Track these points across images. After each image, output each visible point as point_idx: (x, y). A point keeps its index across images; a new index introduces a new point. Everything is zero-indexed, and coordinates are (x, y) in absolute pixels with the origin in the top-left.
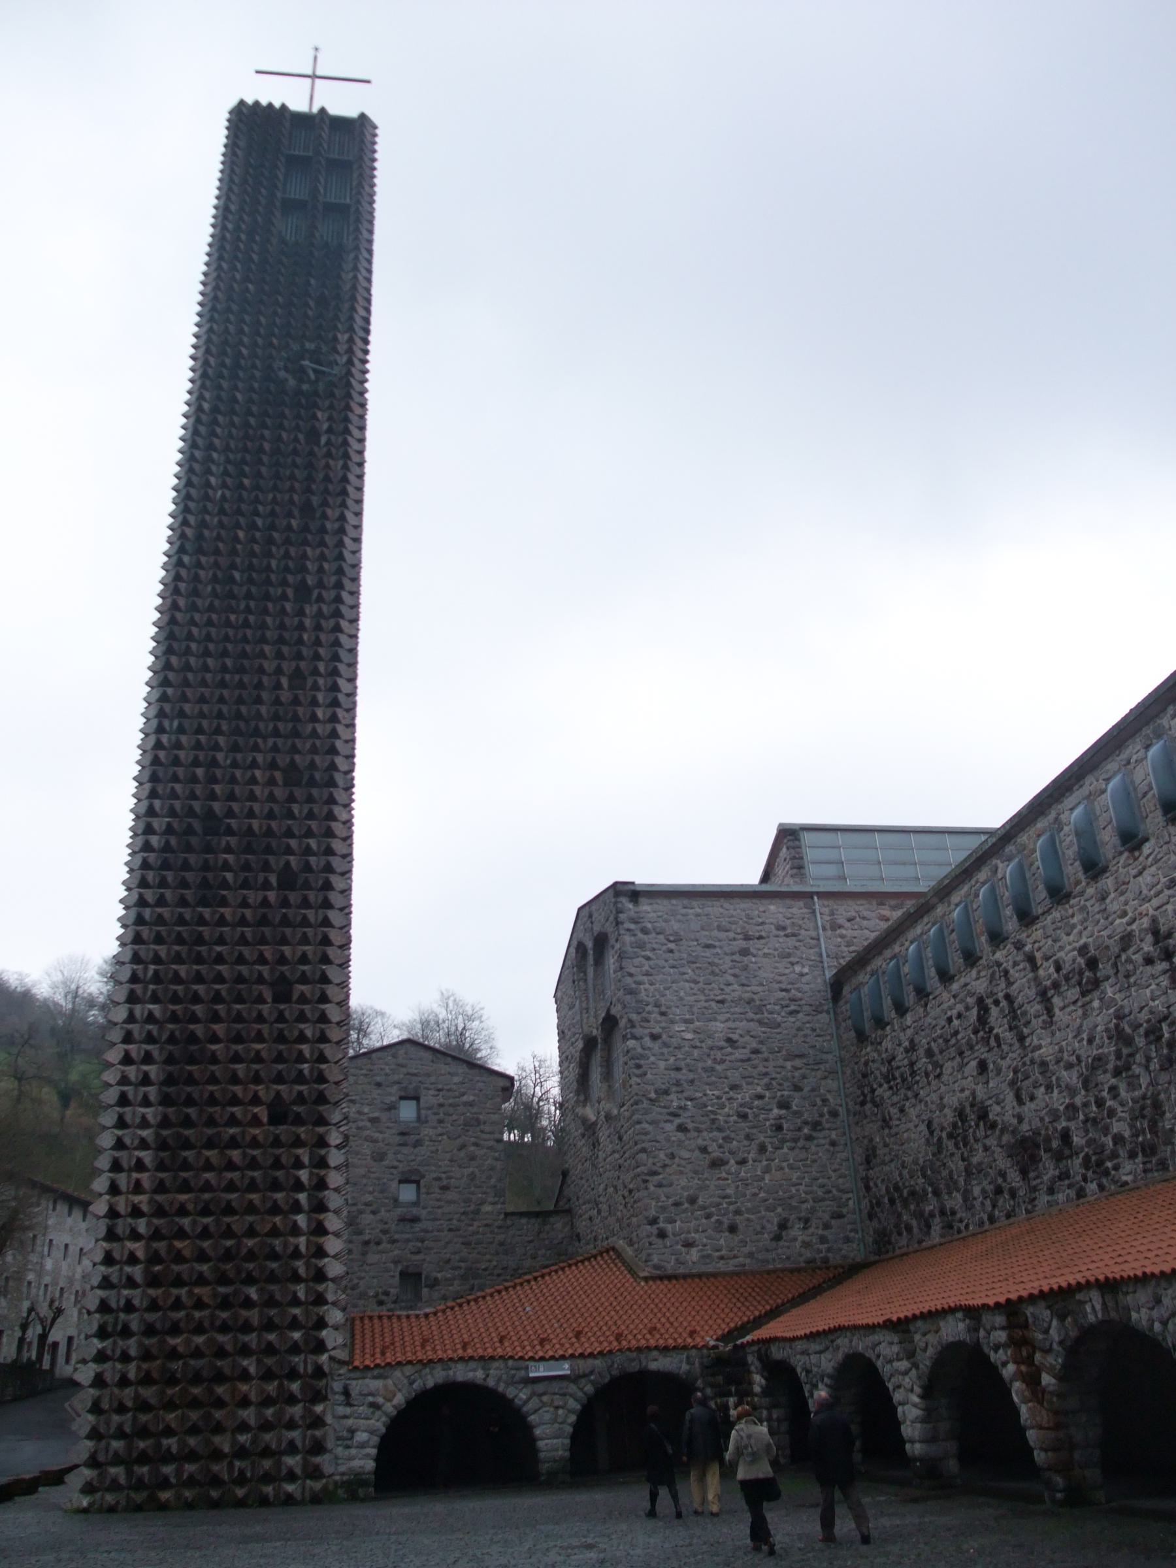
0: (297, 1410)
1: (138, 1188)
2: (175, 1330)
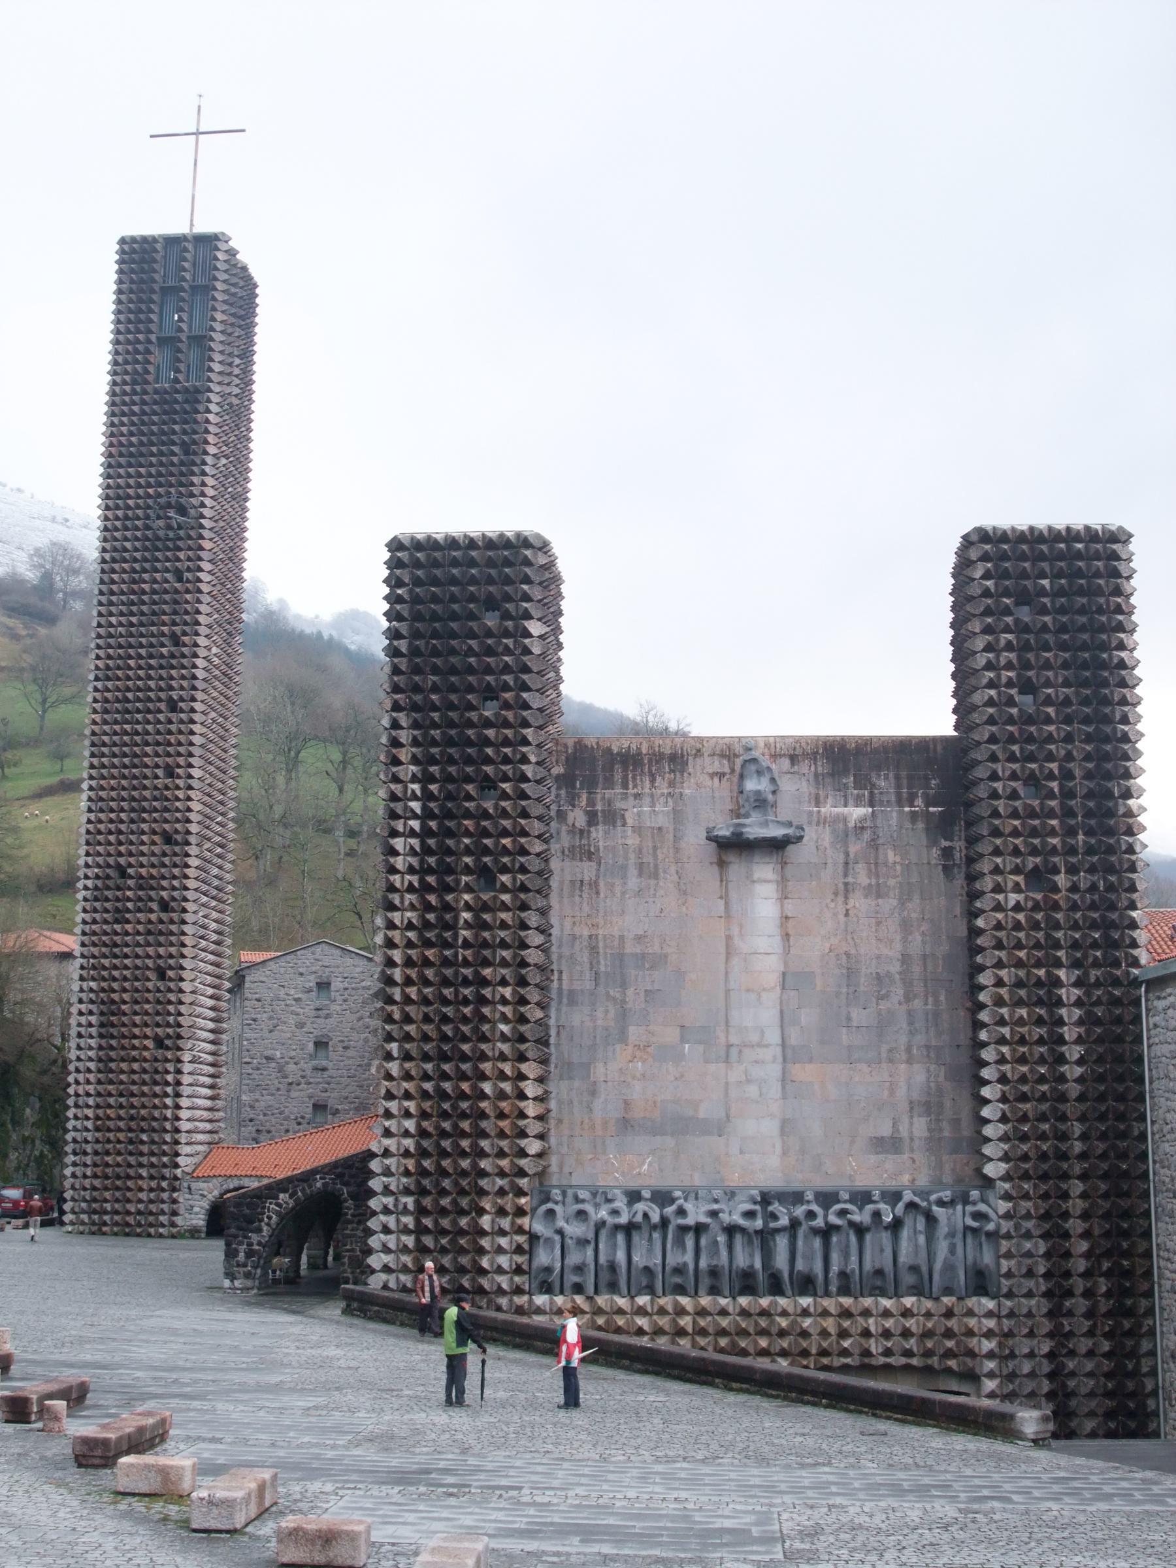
0: (165, 1196)
1: (88, 1082)
2: (108, 1153)
